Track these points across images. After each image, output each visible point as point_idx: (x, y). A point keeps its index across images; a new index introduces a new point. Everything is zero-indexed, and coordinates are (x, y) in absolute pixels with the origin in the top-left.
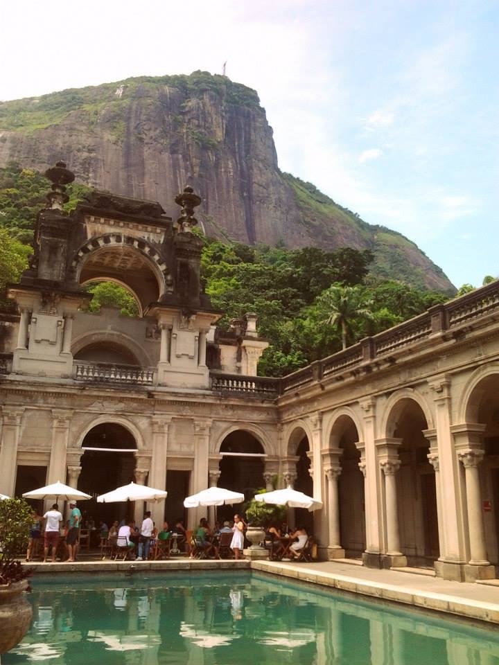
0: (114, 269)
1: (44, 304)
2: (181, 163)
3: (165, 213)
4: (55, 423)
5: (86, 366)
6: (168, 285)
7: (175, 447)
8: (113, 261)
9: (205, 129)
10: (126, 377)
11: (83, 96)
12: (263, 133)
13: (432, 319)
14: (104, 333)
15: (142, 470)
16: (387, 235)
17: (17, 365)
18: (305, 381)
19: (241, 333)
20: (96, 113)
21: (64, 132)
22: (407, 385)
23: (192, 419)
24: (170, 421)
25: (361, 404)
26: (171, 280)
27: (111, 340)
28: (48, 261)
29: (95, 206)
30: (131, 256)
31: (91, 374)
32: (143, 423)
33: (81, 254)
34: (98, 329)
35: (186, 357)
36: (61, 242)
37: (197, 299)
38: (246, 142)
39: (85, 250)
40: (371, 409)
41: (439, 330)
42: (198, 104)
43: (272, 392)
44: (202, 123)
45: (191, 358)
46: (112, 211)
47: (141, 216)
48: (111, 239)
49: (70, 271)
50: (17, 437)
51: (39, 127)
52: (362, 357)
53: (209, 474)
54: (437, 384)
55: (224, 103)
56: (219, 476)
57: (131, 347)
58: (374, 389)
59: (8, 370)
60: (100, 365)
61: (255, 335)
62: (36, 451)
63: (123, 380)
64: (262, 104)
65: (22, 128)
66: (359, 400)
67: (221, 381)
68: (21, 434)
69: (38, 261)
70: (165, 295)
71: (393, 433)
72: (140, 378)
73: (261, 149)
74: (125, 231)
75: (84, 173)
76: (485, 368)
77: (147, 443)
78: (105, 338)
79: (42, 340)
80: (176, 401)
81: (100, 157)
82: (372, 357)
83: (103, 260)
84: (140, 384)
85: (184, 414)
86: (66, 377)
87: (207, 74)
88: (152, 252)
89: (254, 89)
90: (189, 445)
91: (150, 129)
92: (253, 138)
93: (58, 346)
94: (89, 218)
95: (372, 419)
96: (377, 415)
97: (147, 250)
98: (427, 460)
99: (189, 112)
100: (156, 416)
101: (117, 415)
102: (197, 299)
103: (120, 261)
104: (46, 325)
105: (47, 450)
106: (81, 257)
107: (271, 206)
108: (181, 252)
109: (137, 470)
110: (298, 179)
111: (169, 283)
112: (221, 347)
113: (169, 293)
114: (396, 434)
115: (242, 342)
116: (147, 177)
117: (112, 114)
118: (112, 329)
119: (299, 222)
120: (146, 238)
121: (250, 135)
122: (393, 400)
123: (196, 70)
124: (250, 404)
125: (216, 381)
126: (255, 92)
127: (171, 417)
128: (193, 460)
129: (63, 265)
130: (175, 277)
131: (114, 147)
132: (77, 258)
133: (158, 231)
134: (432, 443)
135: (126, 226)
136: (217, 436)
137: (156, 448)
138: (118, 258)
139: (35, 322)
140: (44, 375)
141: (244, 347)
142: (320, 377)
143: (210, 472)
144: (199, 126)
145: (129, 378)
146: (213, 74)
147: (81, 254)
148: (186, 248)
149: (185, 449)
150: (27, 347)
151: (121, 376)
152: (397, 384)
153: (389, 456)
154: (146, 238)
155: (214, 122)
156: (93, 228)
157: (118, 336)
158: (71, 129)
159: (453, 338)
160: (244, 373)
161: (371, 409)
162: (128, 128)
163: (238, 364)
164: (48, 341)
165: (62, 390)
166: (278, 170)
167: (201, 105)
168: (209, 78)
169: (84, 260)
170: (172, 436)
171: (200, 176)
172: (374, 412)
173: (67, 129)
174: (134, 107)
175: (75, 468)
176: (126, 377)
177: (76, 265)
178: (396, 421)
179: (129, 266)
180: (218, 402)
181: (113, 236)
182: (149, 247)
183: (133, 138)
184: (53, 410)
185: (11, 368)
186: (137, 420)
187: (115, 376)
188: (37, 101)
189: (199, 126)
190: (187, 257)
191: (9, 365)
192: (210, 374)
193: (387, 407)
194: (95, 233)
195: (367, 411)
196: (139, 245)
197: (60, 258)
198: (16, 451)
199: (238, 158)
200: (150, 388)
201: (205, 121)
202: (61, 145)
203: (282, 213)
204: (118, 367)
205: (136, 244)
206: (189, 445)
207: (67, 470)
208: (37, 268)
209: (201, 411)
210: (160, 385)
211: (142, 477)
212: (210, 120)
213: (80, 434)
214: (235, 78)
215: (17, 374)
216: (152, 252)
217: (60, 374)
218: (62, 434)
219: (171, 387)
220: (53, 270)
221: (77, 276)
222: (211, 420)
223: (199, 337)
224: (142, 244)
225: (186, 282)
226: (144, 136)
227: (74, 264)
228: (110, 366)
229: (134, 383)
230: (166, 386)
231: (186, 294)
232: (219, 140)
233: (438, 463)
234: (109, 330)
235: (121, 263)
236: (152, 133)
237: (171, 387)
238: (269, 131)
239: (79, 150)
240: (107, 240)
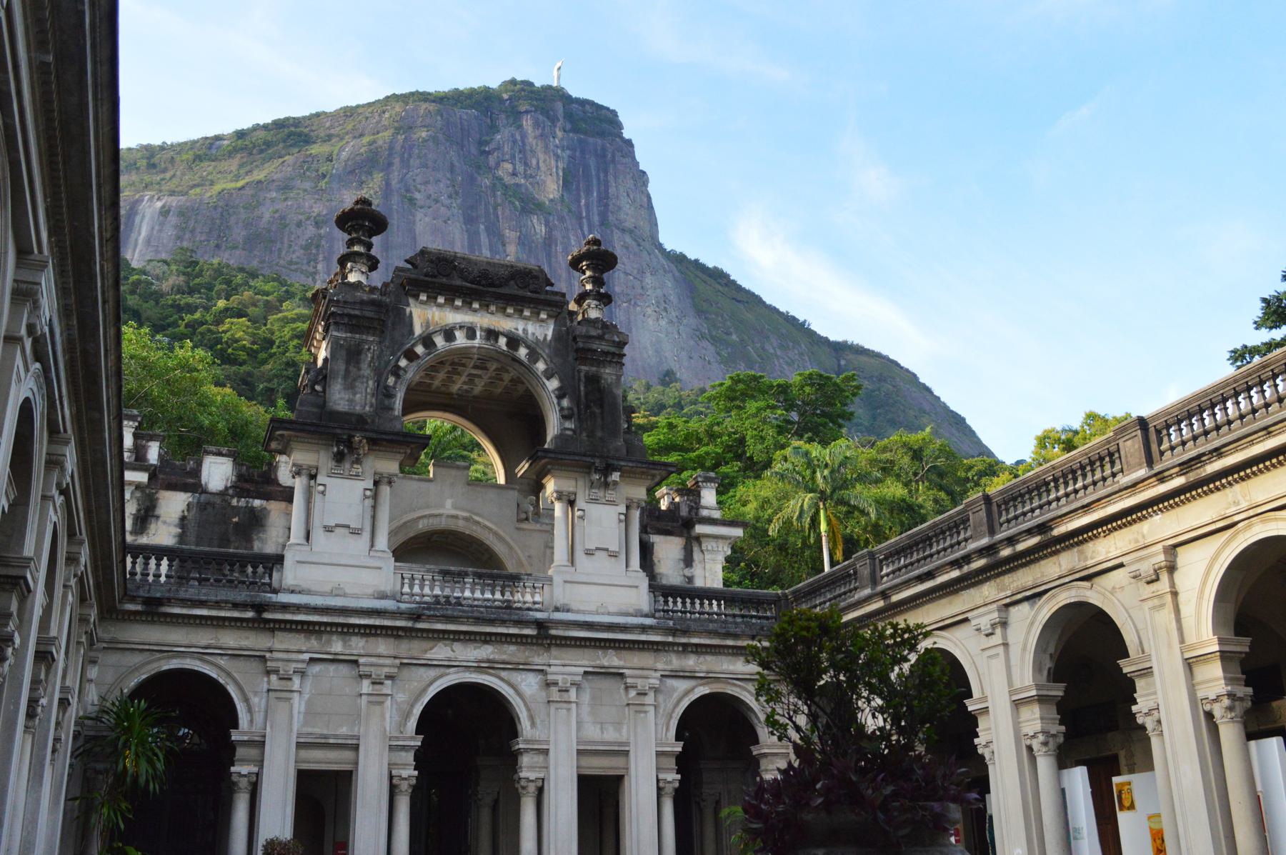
0: (450, 394)
1: (339, 458)
2: (484, 238)
3: (552, 285)
4: (366, 686)
5: (418, 576)
6: (565, 417)
7: (593, 733)
8: (449, 380)
9: (525, 177)
10: (493, 594)
12: (630, 183)
13: (1121, 442)
14: (440, 515)
15: (532, 776)
16: (863, 358)
17: (291, 574)
18: (838, 592)
19: (690, 511)
20: (330, 159)
21: (274, 195)
22: (1077, 576)
23: (621, 675)
24: (579, 678)
25: (973, 622)
26: (569, 409)
27: (453, 527)
28: (346, 376)
29: (426, 275)
30: (486, 369)
31: (427, 590)
32: (529, 684)
33: (403, 363)
34: (428, 507)
35: (604, 554)
36: (366, 342)
37: (620, 442)
38: (600, 199)
39: (411, 356)
40: (998, 631)
41: (1140, 466)
43: (767, 618)
44: (520, 168)
45: (614, 555)
46: (458, 282)
47: (512, 289)
48: (458, 334)
49: (386, 393)
50: (295, 712)
52: (969, 534)
53: (658, 781)
54: (1146, 568)
55: (559, 134)
56: (677, 785)
57: (490, 540)
58: (1002, 590)
59: (275, 584)
60: (445, 573)
61: (717, 515)
62: (331, 741)
63: (488, 600)
64: (626, 134)
65: (198, 190)
66: (969, 615)
67: (670, 599)
68: (303, 709)
69: (325, 377)
70: (560, 437)
71: (1045, 673)
72: (518, 597)
73: (627, 213)
74: (483, 320)
75: (308, 263)
76: (1249, 526)
77: (538, 721)
78: (443, 524)
79: (337, 526)
80: (590, 639)
82: (992, 532)
83: (432, 378)
84: (520, 609)
85: (606, 664)
86: (383, 596)
87: (528, 84)
88: (534, 356)
89: (612, 108)
90: (618, 725)
91: (427, 183)
92: (612, 190)
93: (366, 535)
94: (416, 297)
95: (1001, 650)
96: (1011, 640)
97: (523, 352)
98: (1133, 716)
100: (553, 669)
101: (479, 669)
102: (620, 442)
103: (463, 378)
104: (344, 494)
105: (352, 737)
106: (405, 370)
107: (649, 311)
108: (590, 355)
109: (522, 775)
110: (697, 261)
111: (566, 412)
112: (656, 539)
113: (569, 433)
114: (1056, 675)
115: (693, 526)
118: (454, 507)
119: (703, 337)
120: (520, 332)
121: (607, 186)
122: (1047, 609)
123: (508, 78)
124: (730, 642)
125: (661, 599)
126: (614, 113)
127: (582, 670)
128: (626, 753)
129: (371, 383)
130: (576, 400)
132: (397, 371)
133: (543, 316)
134: (1140, 684)
135: (485, 307)
136: (670, 705)
137: (560, 730)
138: (459, 374)
139: (323, 493)
140: (340, 592)
141: (698, 539)
142: (874, 581)
143: (661, 776)
144: (514, 174)
145: (498, 596)
147: (403, 363)
148: (595, 347)
149: (610, 735)
150: (308, 538)
151: (483, 593)
152: (1056, 576)
153: (1042, 718)
154: (520, 332)
156: (425, 315)
157: (466, 519)
158: (286, 187)
159: (1179, 474)
160: (699, 583)
161: (998, 631)
162: (388, 184)
163: (688, 572)
164: (348, 527)
165: (378, 622)
166: (660, 247)
167: (518, 137)
168: (532, 92)
169: (409, 375)
170: (585, 709)
172: (1004, 636)
173: (279, 189)
174: (398, 147)
175: (405, 773)
176: (493, 594)
177: (396, 383)
178: (1051, 649)
179: (478, 389)
180: (670, 639)
181: (461, 327)
182: (528, 347)
184: (362, 660)
185: (281, 581)
186: (517, 677)
187: (473, 592)
189: (514, 174)
190: (599, 363)
191: (275, 575)
192: (650, 586)
193: (1032, 623)
194: (427, 324)
195: (987, 635)
196: (508, 344)
197: (366, 371)
198: (294, 740)
200: (539, 615)
202: (267, 216)
203: (671, 322)
204: (480, 576)
205: (502, 341)
206: (618, 725)
207: (391, 777)
208: (324, 391)
209: (637, 659)
210: (557, 609)
211: (532, 788)
212: (534, 162)
213: (412, 706)
214: (575, 91)
215: (293, 592)
216: (534, 356)
217: (370, 591)
218: (377, 708)
219: (578, 612)
220: (354, 394)
221: (398, 404)
222: (658, 674)
223: (626, 515)
224: (514, 342)
225: (598, 411)
226: (417, 196)
227: (391, 381)
228: (462, 575)
229: (508, 606)
230: (568, 611)
231: (599, 434)
232: (551, 196)
233: (1159, 722)
234: (448, 508)
235: (465, 383)
236: (431, 189)
237: (578, 612)
238: (641, 178)
239: (299, 224)
240: (449, 335)
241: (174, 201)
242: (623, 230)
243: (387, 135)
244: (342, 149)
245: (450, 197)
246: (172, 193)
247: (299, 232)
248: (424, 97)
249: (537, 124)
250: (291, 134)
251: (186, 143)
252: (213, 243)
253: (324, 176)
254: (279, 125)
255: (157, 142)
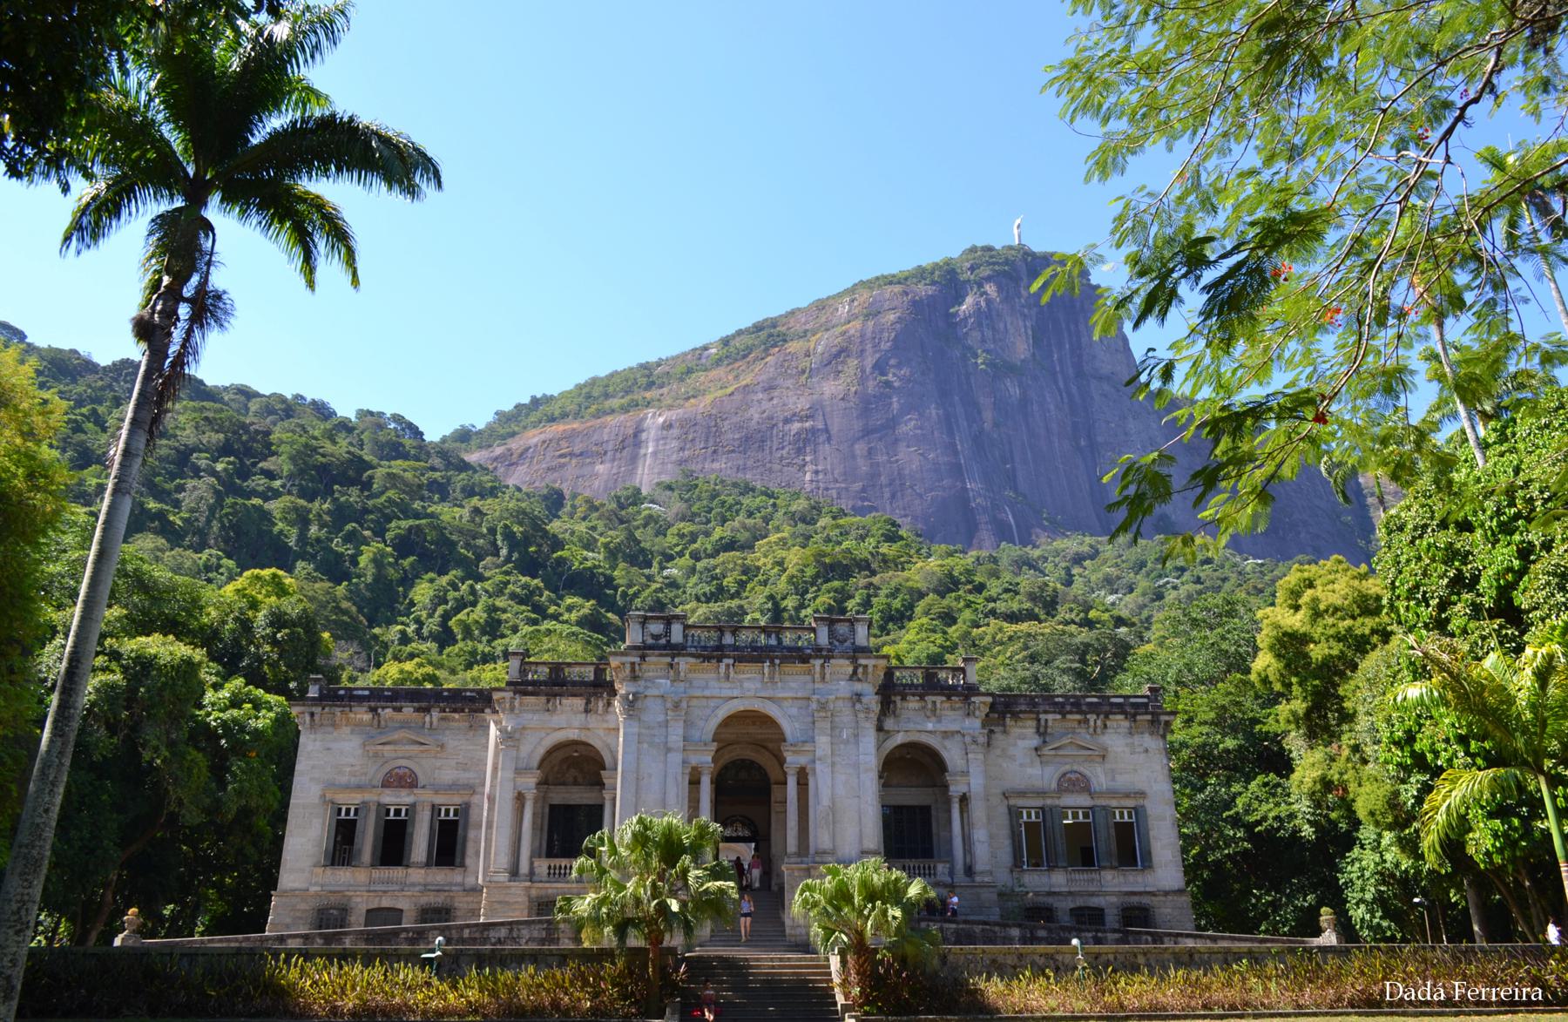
9: (994, 341)
11: (783, 329)
21: (760, 396)
42: (978, 303)
44: (988, 333)
51: (720, 393)
81: (820, 426)
87: (989, 249)
99: (966, 318)
116: (902, 447)
117: (834, 350)
123: (968, 246)
131: (842, 404)
146: (998, 247)
155: (1012, 331)
158: (770, 388)
162: (863, 371)
167: (983, 304)
171: (996, 425)
183: (871, 384)
188: (714, 351)
199: (1061, 384)
201: (994, 329)
212: (1002, 326)
226: (890, 377)
239: (787, 421)
241: (673, 415)
242: (1100, 378)
243: (856, 325)
244: (818, 343)
245: (923, 374)
246: (670, 408)
247: (787, 427)
248: (890, 280)
249: (1000, 289)
250: (769, 335)
251: (678, 357)
252: (710, 450)
253: (803, 372)
254: (758, 328)
255: (653, 359)
